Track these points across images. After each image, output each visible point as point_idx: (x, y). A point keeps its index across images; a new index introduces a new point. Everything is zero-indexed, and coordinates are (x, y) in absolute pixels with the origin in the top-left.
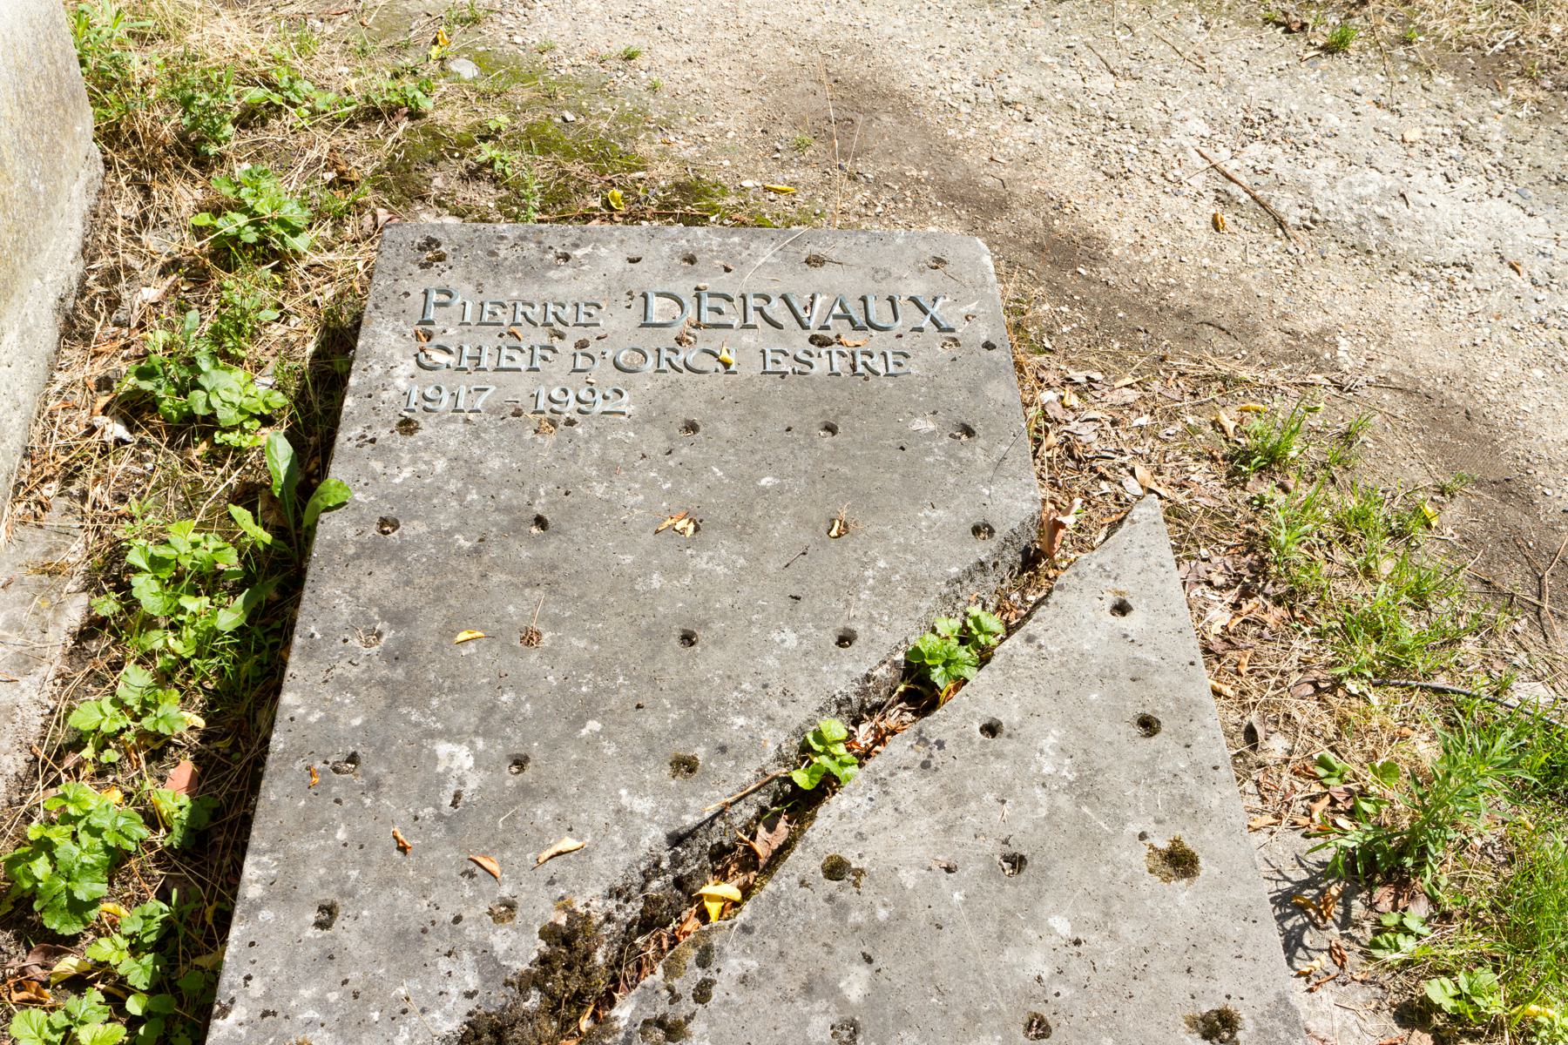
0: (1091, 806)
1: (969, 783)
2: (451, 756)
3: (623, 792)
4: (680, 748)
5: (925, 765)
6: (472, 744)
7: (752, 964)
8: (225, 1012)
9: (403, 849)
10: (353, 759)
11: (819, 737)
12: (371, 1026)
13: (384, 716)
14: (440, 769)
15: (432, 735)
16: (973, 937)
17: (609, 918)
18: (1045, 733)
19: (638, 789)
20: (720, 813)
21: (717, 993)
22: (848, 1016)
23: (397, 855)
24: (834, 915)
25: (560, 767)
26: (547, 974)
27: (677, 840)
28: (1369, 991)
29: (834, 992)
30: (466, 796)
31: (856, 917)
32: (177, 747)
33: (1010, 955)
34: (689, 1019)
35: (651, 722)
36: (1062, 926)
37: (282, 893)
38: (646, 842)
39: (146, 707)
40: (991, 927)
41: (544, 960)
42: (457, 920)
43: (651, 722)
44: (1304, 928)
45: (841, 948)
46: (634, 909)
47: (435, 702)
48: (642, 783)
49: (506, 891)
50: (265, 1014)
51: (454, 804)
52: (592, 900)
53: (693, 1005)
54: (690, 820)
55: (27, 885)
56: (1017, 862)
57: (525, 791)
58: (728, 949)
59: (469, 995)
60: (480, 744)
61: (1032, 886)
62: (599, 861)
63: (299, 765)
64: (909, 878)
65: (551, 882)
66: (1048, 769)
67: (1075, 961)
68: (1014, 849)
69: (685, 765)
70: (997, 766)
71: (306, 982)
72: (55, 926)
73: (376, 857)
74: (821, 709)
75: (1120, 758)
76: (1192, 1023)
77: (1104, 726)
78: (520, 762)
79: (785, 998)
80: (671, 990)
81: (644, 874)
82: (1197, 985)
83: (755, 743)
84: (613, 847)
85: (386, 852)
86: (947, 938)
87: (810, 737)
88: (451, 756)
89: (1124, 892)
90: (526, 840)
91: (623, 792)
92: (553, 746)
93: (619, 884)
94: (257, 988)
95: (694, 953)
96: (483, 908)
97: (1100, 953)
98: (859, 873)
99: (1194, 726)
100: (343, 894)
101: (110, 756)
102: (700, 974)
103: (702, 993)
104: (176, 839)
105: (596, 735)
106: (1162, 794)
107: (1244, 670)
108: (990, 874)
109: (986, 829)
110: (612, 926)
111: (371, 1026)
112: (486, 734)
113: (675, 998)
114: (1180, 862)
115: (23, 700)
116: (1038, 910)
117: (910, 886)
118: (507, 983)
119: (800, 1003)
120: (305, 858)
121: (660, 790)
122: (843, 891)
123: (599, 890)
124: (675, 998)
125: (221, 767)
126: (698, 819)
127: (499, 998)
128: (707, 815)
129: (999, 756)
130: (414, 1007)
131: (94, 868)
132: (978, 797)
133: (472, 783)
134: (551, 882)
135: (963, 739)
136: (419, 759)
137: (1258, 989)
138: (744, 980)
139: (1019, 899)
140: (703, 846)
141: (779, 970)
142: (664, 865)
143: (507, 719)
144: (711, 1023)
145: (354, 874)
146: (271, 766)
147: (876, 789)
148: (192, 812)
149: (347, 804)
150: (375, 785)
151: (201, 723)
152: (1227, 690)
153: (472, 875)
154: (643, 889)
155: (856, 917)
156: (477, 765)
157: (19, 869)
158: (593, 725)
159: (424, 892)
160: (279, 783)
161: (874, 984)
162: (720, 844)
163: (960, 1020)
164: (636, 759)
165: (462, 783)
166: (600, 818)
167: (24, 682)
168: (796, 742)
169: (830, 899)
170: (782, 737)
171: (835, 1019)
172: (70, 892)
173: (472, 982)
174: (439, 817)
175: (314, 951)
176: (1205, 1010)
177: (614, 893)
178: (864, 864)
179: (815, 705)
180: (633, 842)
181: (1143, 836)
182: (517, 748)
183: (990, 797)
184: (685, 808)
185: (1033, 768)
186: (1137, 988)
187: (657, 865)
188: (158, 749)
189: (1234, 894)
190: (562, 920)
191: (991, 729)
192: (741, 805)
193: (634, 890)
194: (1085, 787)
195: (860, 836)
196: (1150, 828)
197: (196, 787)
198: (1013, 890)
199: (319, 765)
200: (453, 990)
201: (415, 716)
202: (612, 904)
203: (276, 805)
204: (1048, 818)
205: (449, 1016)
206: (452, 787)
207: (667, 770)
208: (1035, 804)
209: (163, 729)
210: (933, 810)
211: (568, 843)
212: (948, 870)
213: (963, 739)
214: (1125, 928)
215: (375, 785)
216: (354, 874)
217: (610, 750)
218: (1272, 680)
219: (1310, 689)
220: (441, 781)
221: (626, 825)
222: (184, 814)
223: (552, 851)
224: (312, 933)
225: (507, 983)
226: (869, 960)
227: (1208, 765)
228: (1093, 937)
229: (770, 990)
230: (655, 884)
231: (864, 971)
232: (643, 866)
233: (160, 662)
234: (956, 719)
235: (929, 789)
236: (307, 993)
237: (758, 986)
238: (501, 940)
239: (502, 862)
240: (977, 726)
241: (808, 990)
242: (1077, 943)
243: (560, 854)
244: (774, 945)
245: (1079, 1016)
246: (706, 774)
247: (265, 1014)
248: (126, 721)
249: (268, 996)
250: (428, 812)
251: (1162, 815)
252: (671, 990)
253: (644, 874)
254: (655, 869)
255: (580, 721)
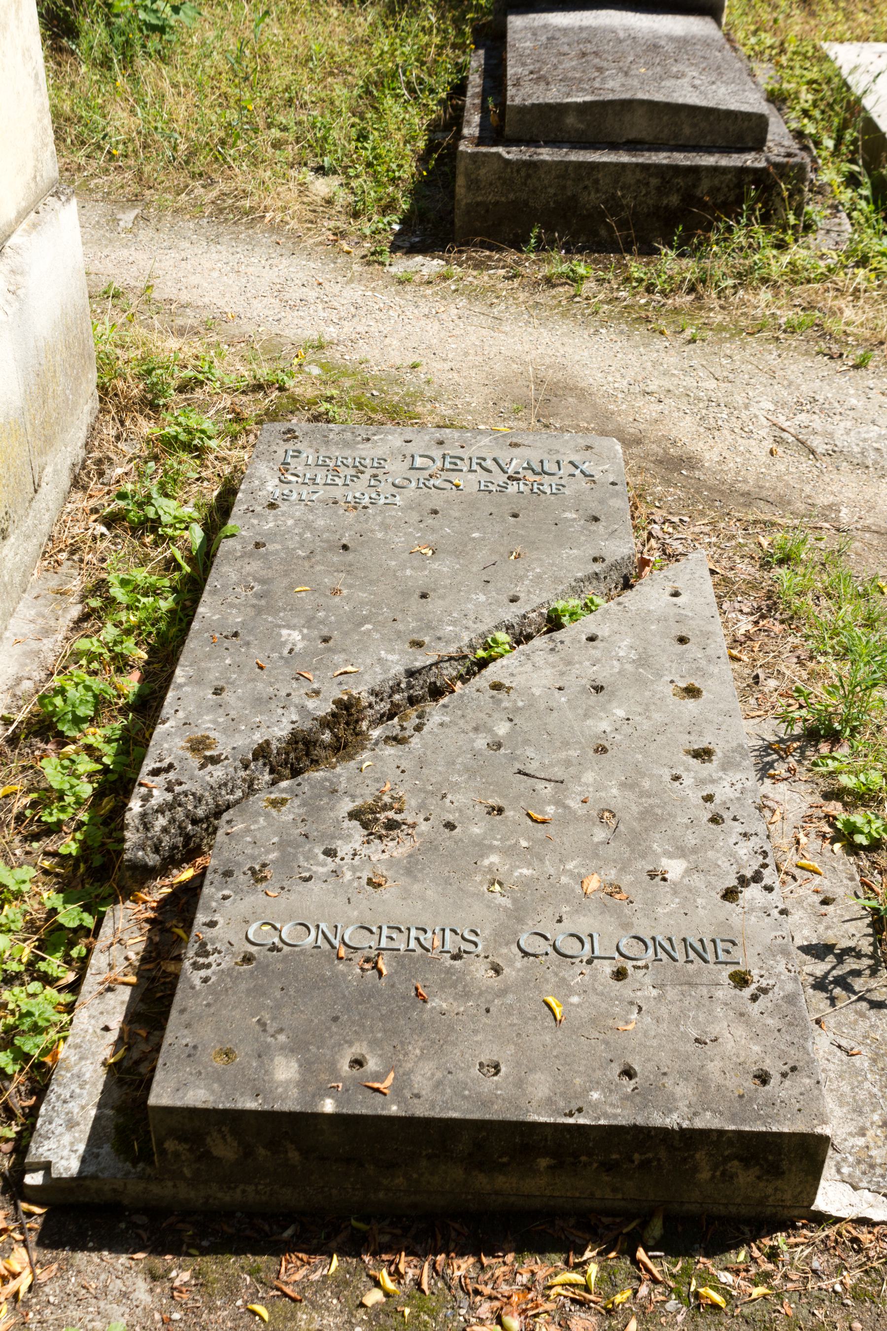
0: (645, 669)
1: (576, 658)
2: (289, 635)
3: (383, 652)
4: (416, 637)
5: (552, 650)
6: (301, 631)
7: (447, 719)
8: (164, 722)
9: (261, 668)
10: (236, 635)
11: (494, 640)
12: (241, 731)
13: (253, 619)
14: (283, 639)
15: (280, 626)
16: (570, 715)
17: (370, 706)
18: (622, 641)
19: (392, 651)
20: (436, 664)
21: (426, 729)
22: (497, 740)
23: (258, 670)
24: (494, 703)
25: (348, 642)
26: (335, 723)
27: (411, 674)
28: (808, 786)
29: (490, 731)
30: (297, 649)
31: (505, 704)
32: (132, 667)
33: (589, 722)
34: (410, 737)
35: (400, 626)
36: (621, 713)
37: (196, 681)
38: (393, 672)
39: (115, 643)
40: (580, 711)
41: (334, 715)
42: (289, 695)
43: (400, 626)
44: (777, 760)
45: (496, 715)
46: (384, 707)
47: (281, 614)
48: (394, 650)
49: (315, 686)
50: (185, 724)
51: (290, 653)
52: (361, 691)
53: (412, 732)
54: (418, 664)
55: (50, 708)
56: (599, 689)
57: (329, 650)
58: (434, 713)
59: (293, 722)
60: (305, 631)
61: (606, 698)
62: (367, 677)
63: (206, 635)
64: (537, 692)
65: (341, 684)
66: (621, 654)
67: (625, 726)
68: (598, 683)
69: (418, 644)
70: (593, 652)
71: (207, 714)
72: (65, 729)
73: (246, 671)
74: (496, 627)
75: (664, 651)
76: (688, 752)
77: (657, 639)
78: (326, 640)
79: (463, 732)
80: (402, 726)
81: (391, 688)
82: (692, 738)
83: (458, 637)
84: (375, 672)
85: (252, 669)
86: (555, 714)
87: (489, 640)
88: (289, 635)
89: (658, 702)
90: (328, 667)
91: (383, 652)
92: (346, 634)
93: (377, 689)
94: (181, 714)
95: (415, 713)
96: (303, 691)
97: (641, 724)
98: (509, 688)
99: (709, 642)
100: (228, 683)
101: (95, 665)
102: (417, 721)
103: (418, 728)
104: (131, 698)
105: (369, 631)
106: (685, 667)
107: (756, 649)
108: (584, 690)
109: (583, 675)
110: (372, 712)
111: (241, 731)
112: (308, 628)
113: (403, 728)
114: (692, 692)
115: (44, 648)
116: (608, 706)
117: (537, 694)
118: (314, 719)
119: (471, 734)
120: (209, 669)
121: (402, 652)
122: (502, 695)
123: (366, 688)
124: (403, 728)
125: (155, 674)
126: (423, 664)
127: (308, 725)
128: (428, 663)
129: (594, 648)
130: (263, 725)
131: (88, 702)
132: (581, 663)
133: (299, 646)
134: (341, 684)
135: (575, 640)
136: (271, 634)
137: (728, 741)
138: (442, 725)
139: (598, 701)
140: (425, 681)
141: (461, 722)
142: (403, 686)
143: (320, 622)
144: (422, 739)
145: (234, 676)
146: (191, 634)
147: (523, 658)
148: (140, 689)
149: (232, 650)
150: (248, 644)
151: (146, 657)
152: (745, 658)
153: (297, 679)
154: (390, 696)
155: (505, 704)
156: (303, 639)
157: (46, 701)
158: (369, 626)
159: (271, 684)
160: (195, 642)
161: (513, 729)
162: (435, 683)
163: (558, 744)
164: (390, 640)
165: (294, 645)
166: (369, 661)
167: (45, 641)
168: (480, 641)
169: (492, 697)
170: (473, 635)
171: (489, 741)
172: (74, 713)
173: (295, 718)
174: (282, 658)
175: (211, 703)
176: (696, 747)
177: (373, 693)
178: (513, 685)
179: (493, 624)
180: (386, 671)
181: (672, 682)
182: (325, 632)
183: (587, 663)
184: (416, 660)
185: (614, 653)
186: (658, 738)
187: (398, 685)
188: (122, 664)
189: (721, 706)
190: (346, 698)
191: (592, 639)
192: (447, 664)
193: (385, 694)
194: (643, 661)
195: (512, 675)
196: (677, 679)
197: (141, 680)
198: (594, 698)
199: (217, 635)
200: (284, 720)
201: (270, 619)
202: (372, 699)
203: (193, 650)
204: (619, 673)
205: (281, 730)
206: (289, 646)
207: (407, 645)
208: (613, 667)
209: (125, 651)
210: (554, 667)
211: (350, 669)
212: (560, 689)
213: (575, 640)
214: (656, 716)
215: (248, 644)
216: (234, 676)
217: (377, 636)
218: (772, 654)
219: (795, 660)
220: (284, 644)
221: (382, 665)
222: (136, 690)
223: (342, 670)
224: (210, 696)
225: (314, 719)
226: (511, 720)
227: (715, 657)
228: (638, 718)
229: (456, 729)
230: (397, 697)
231: (508, 724)
232: (391, 683)
233: (125, 626)
234: (573, 633)
235: (552, 658)
236: (206, 718)
237: (448, 726)
238: (311, 704)
239: (314, 676)
240: (584, 637)
241: (476, 729)
242: (628, 719)
243: (346, 673)
244: (460, 712)
245: (623, 746)
246: (429, 647)
247: (185, 724)
248: (105, 651)
249: (187, 717)
250: (275, 655)
251: (684, 673)
252: (402, 726)
253: (391, 688)
254: (396, 688)
255: (361, 624)
